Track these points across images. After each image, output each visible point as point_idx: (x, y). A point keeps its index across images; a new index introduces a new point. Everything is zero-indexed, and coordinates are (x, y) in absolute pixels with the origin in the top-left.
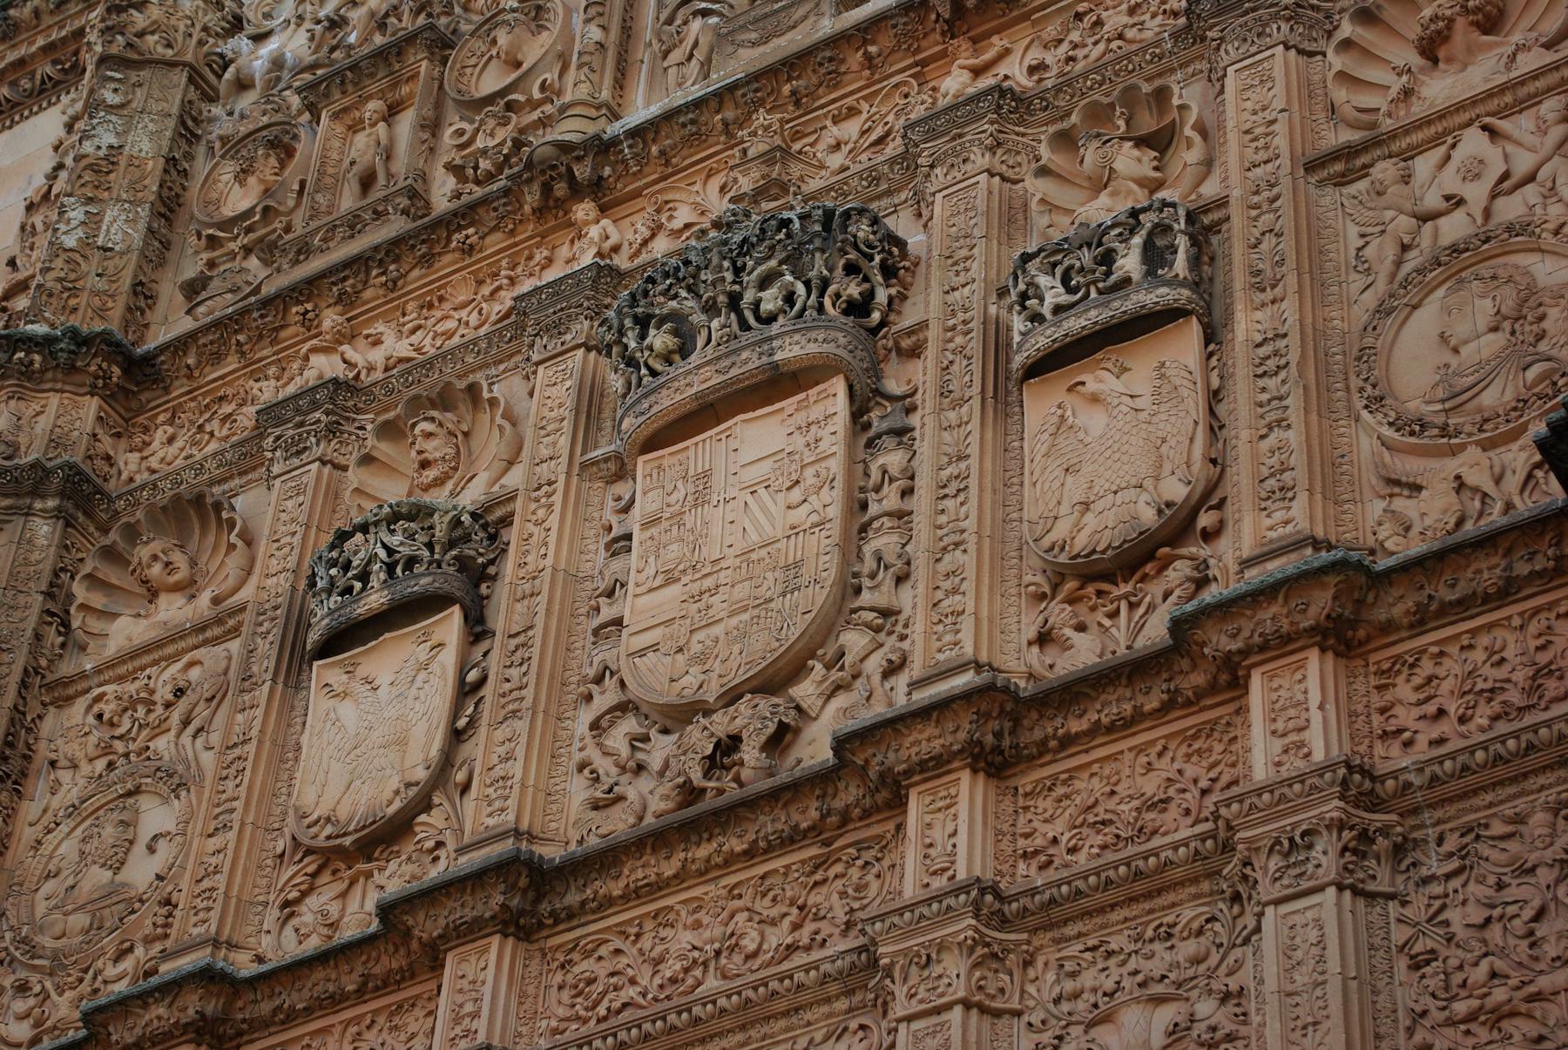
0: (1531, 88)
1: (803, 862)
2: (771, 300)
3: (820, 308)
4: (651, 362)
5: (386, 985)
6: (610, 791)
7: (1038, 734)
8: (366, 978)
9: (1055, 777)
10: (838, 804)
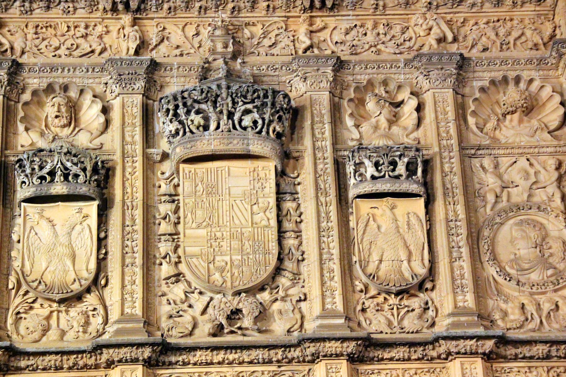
0: (545, 150)
1: (269, 371)
2: (247, 121)
3: (268, 133)
4: (191, 127)
5: (82, 368)
6: (178, 312)
7: (371, 355)
8: (75, 364)
9: (373, 370)
10: (289, 356)
